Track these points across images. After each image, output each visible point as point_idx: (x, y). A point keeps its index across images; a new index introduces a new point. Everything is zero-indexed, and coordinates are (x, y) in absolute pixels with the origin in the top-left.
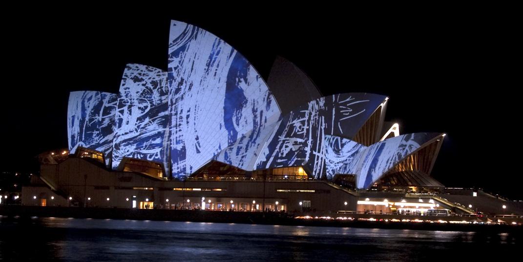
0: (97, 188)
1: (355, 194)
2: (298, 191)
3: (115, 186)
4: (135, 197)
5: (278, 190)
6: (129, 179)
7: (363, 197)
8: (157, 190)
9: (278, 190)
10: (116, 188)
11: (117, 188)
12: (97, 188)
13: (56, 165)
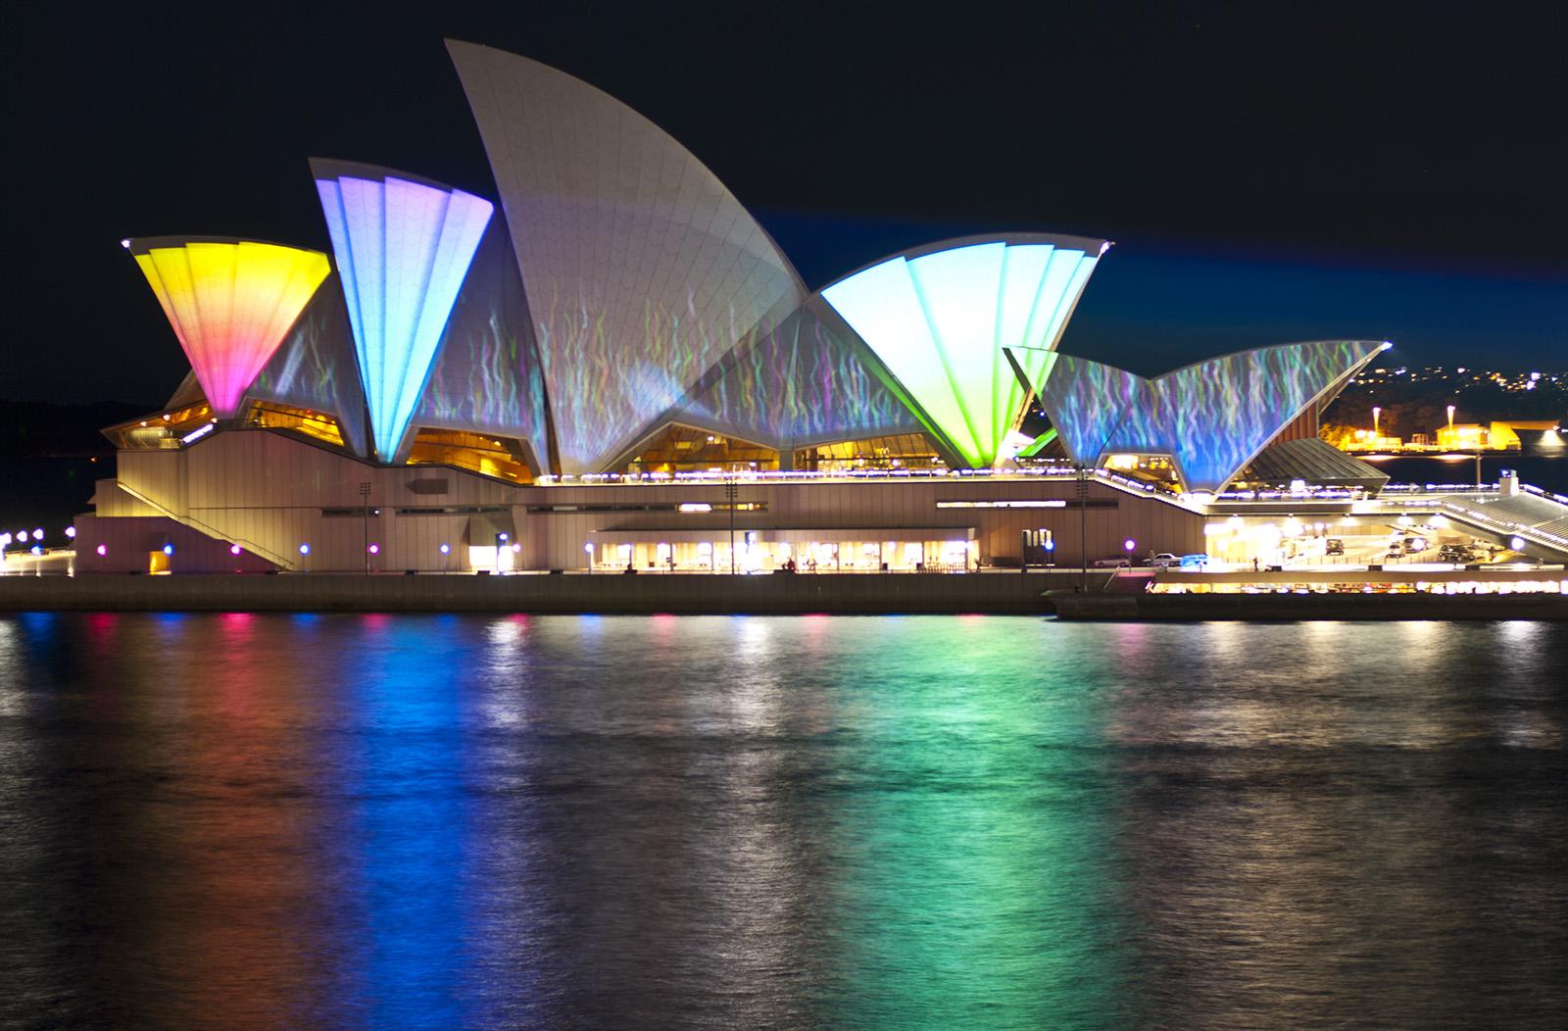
0: (329, 512)
1: (1196, 502)
2: (995, 504)
3: (395, 507)
4: (503, 537)
5: (940, 505)
6: (441, 487)
7: (1222, 512)
8: (525, 510)
9: (940, 505)
10: (397, 514)
11: (405, 511)
12: (329, 512)
13: (174, 450)
